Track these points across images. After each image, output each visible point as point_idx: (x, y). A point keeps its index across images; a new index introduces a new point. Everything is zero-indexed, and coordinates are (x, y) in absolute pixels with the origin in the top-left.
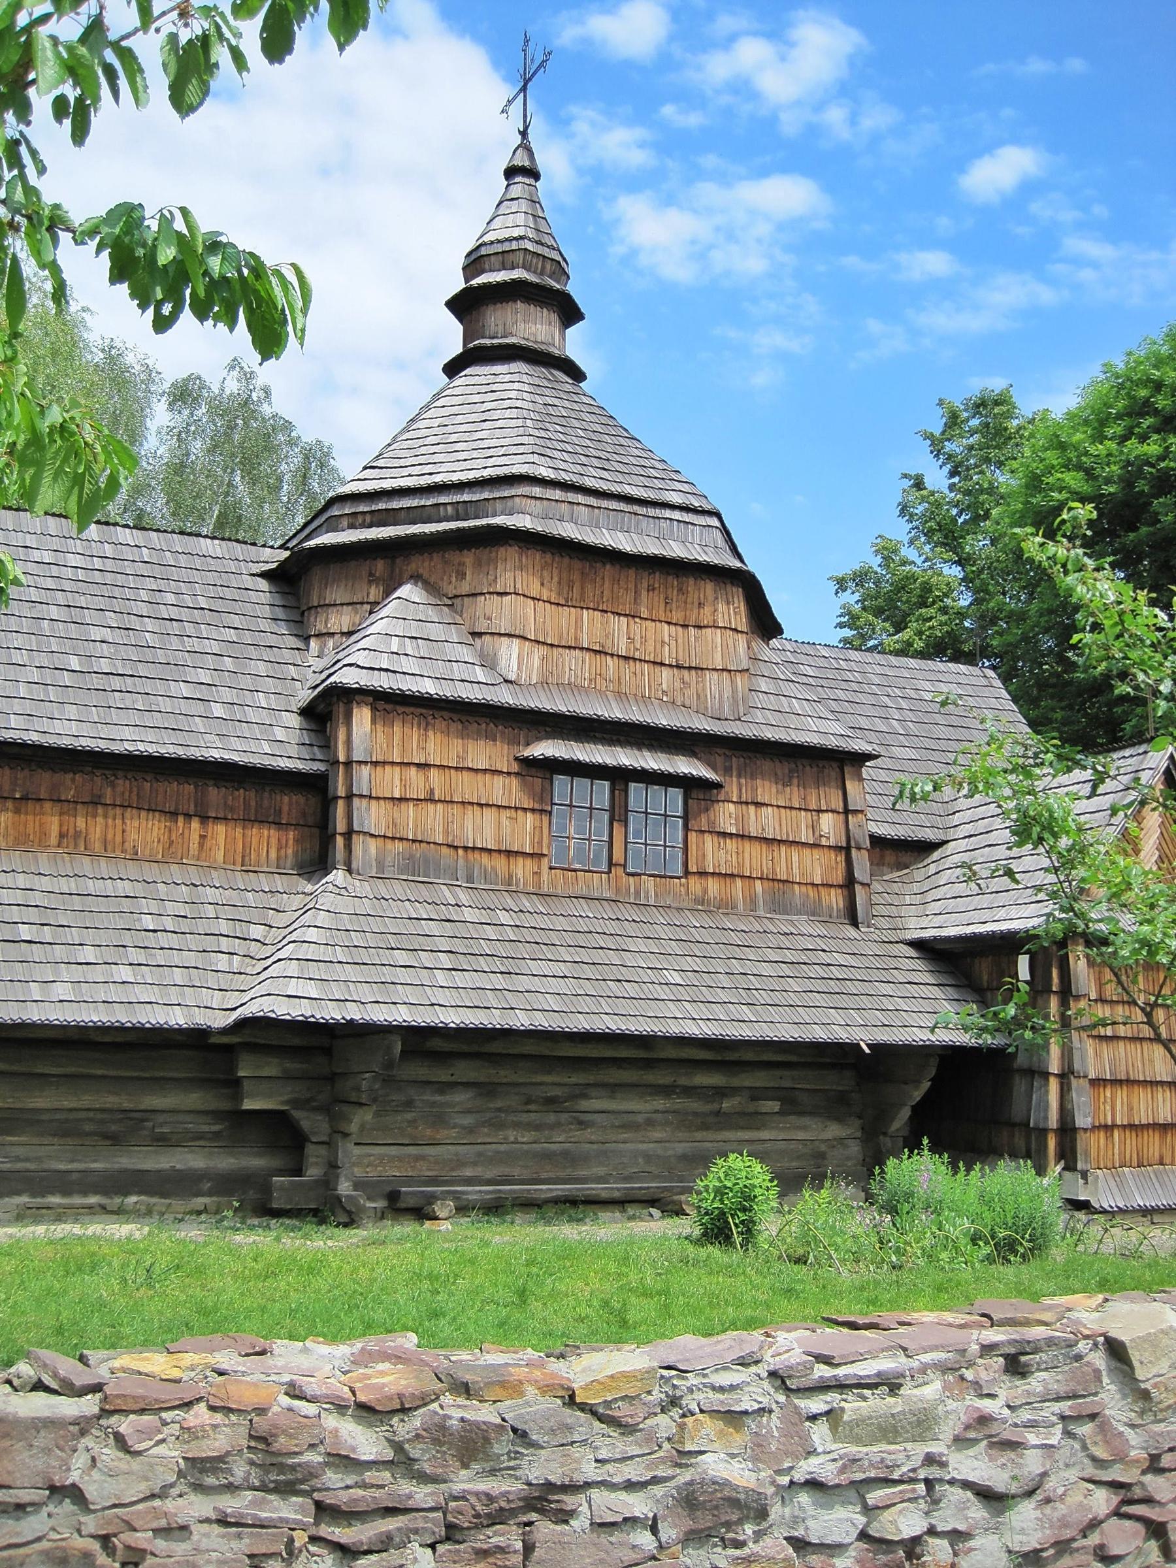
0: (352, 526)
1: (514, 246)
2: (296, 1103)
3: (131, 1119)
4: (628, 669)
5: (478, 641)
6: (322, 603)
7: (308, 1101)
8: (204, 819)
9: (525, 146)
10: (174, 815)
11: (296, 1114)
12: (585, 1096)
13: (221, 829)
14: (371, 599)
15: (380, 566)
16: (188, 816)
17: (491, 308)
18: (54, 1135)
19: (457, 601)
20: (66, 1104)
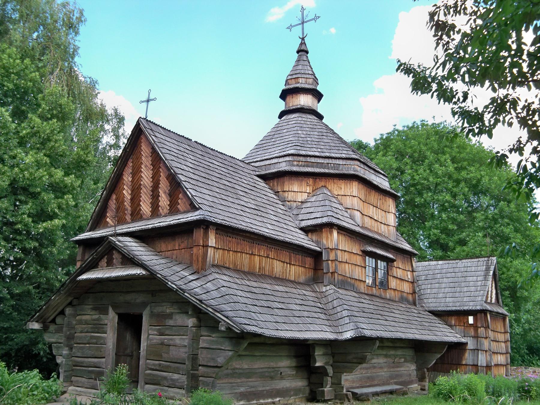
0: (298, 165)
1: (310, 76)
2: (327, 363)
3: (276, 371)
4: (376, 222)
5: (349, 211)
6: (290, 190)
7: (329, 362)
8: (290, 264)
9: (303, 43)
10: (284, 262)
11: (327, 367)
12: (373, 358)
13: (293, 268)
14: (308, 192)
15: (311, 181)
16: (287, 263)
17: (302, 95)
18: (260, 378)
19: (339, 197)
20: (262, 366)
